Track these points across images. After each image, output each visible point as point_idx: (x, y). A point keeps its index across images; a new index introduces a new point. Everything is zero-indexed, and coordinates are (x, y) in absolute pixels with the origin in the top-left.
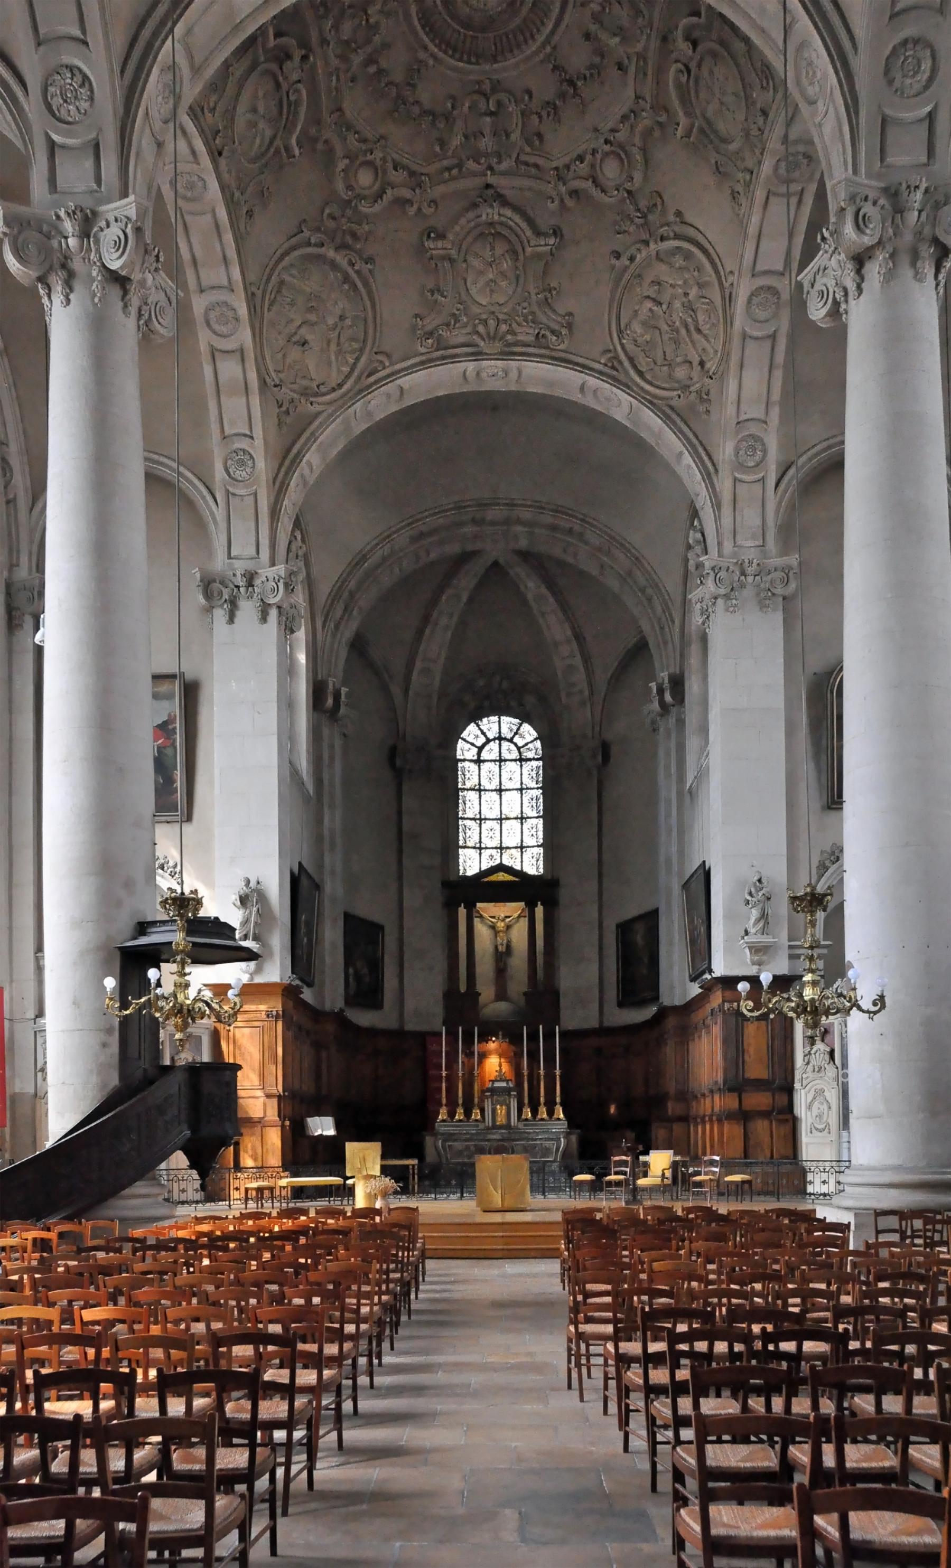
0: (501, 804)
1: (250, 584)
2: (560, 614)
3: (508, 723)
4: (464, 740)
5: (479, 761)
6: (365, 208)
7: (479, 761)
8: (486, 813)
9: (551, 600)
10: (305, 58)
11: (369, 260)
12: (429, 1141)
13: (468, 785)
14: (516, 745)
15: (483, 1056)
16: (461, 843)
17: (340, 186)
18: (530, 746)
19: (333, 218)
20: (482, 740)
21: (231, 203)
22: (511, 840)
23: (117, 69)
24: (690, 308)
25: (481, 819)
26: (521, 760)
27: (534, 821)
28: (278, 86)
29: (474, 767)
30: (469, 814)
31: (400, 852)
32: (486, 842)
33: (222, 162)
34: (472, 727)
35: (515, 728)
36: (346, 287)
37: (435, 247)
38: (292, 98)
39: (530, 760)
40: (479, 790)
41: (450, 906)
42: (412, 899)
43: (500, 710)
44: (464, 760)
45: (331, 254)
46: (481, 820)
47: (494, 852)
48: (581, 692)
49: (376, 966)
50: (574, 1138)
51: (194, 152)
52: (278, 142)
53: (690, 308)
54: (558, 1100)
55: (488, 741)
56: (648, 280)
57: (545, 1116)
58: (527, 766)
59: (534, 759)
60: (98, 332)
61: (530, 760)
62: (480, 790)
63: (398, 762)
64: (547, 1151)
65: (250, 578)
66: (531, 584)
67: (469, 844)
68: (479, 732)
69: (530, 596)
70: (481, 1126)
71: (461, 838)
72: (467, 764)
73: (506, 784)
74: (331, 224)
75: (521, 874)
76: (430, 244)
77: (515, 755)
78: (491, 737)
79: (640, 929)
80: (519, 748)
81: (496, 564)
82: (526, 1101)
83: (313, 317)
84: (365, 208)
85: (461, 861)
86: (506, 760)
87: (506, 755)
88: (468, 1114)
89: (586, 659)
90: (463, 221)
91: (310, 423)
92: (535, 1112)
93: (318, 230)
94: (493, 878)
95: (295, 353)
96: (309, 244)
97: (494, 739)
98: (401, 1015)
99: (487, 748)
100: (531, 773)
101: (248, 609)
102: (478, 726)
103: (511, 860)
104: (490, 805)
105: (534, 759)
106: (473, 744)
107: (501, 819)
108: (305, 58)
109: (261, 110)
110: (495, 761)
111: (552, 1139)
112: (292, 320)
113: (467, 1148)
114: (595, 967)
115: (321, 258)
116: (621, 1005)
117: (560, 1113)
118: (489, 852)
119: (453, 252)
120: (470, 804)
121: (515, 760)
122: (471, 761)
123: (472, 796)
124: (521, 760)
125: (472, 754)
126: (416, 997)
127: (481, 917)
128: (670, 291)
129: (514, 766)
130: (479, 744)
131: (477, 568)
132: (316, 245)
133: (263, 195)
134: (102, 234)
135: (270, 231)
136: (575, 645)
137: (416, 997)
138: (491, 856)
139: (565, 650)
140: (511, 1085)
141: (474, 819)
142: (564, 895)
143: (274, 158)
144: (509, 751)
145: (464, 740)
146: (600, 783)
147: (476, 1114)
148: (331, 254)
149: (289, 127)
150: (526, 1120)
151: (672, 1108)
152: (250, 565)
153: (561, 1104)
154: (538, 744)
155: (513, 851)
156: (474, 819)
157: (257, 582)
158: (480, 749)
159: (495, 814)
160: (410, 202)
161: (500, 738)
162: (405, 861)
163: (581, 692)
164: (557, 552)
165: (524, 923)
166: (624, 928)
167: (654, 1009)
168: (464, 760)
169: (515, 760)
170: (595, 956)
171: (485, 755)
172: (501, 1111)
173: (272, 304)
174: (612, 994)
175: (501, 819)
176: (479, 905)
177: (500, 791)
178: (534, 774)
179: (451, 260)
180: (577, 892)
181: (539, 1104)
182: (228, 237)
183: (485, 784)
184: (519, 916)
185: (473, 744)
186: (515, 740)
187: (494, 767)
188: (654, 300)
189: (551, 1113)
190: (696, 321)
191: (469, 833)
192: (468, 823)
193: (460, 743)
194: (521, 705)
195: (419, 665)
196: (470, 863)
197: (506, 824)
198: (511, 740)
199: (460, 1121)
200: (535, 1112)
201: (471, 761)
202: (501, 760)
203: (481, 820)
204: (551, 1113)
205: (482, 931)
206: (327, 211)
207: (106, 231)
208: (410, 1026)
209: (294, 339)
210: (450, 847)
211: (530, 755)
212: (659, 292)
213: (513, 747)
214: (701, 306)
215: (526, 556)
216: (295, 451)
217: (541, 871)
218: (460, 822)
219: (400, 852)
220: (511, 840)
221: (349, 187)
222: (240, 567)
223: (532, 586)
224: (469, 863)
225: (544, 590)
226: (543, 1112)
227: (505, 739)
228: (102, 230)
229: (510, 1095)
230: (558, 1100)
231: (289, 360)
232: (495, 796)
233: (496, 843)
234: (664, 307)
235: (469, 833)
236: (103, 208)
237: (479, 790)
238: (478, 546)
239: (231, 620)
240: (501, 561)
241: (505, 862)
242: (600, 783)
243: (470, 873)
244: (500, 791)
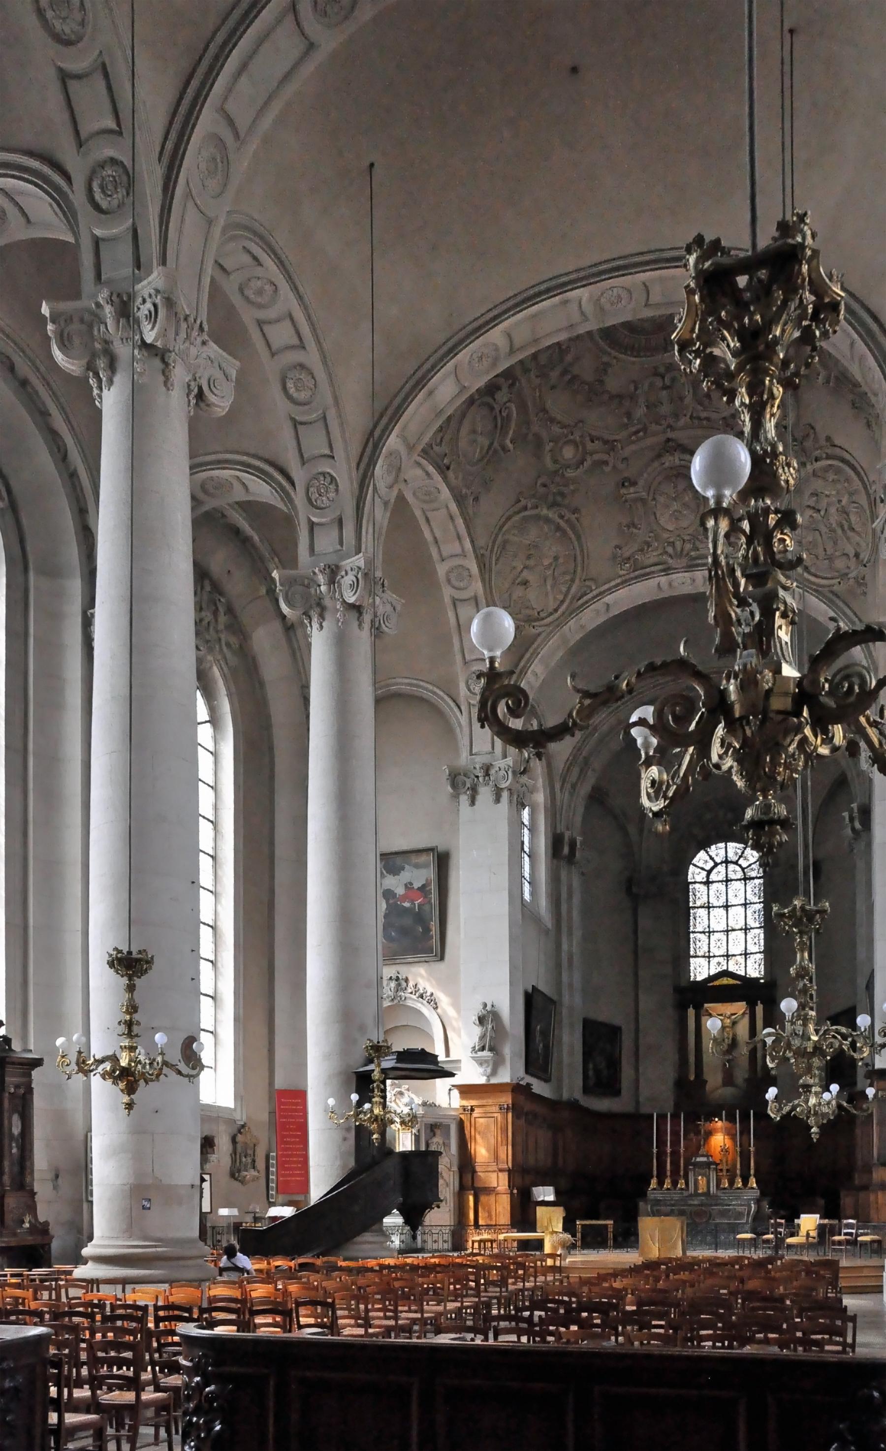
0: (726, 919)
1: (487, 774)
6: (570, 473)
8: (714, 926)
10: (512, 386)
11: (576, 511)
16: (692, 953)
17: (548, 460)
18: (753, 866)
19: (545, 486)
21: (460, 499)
23: (354, 465)
24: (845, 512)
25: (709, 932)
28: (492, 409)
30: (699, 928)
32: (714, 951)
33: (451, 474)
36: (558, 534)
37: (630, 492)
38: (504, 414)
40: (708, 907)
42: (646, 1002)
45: (545, 512)
46: (709, 933)
51: (428, 474)
52: (496, 444)
53: (845, 512)
56: (807, 494)
58: (750, 885)
60: (341, 645)
62: (709, 908)
65: (487, 769)
71: (692, 949)
74: (542, 490)
76: (623, 491)
83: (531, 562)
84: (570, 473)
85: (692, 968)
86: (731, 880)
90: (650, 469)
91: (535, 640)
93: (534, 496)
95: (518, 592)
96: (525, 508)
101: (485, 794)
107: (727, 931)
108: (512, 386)
109: (479, 430)
112: (514, 568)
115: (538, 517)
119: (644, 494)
120: (699, 920)
123: (702, 912)
124: (746, 879)
126: (650, 1083)
128: (826, 500)
129: (739, 885)
132: (532, 508)
133: (486, 484)
134: (342, 581)
135: (493, 506)
137: (650, 1083)
141: (704, 932)
143: (492, 456)
148: (545, 512)
149: (504, 433)
152: (485, 759)
156: (704, 932)
157: (492, 772)
159: (723, 927)
160: (606, 463)
162: (641, 973)
173: (497, 560)
175: (727, 931)
177: (727, 907)
179: (643, 501)
182: (460, 521)
183: (713, 901)
187: (722, 887)
188: (814, 508)
190: (849, 521)
192: (699, 936)
196: (700, 970)
197: (732, 935)
203: (709, 933)
206: (539, 482)
207: (346, 578)
209: (519, 580)
210: (681, 956)
212: (817, 502)
214: (852, 509)
216: (522, 664)
218: (692, 936)
221: (555, 462)
222: (479, 761)
224: (699, 969)
228: (343, 577)
231: (514, 597)
232: (722, 911)
233: (723, 951)
234: (822, 513)
235: (699, 943)
236: (343, 563)
239: (473, 802)
243: (699, 979)
244: (727, 907)
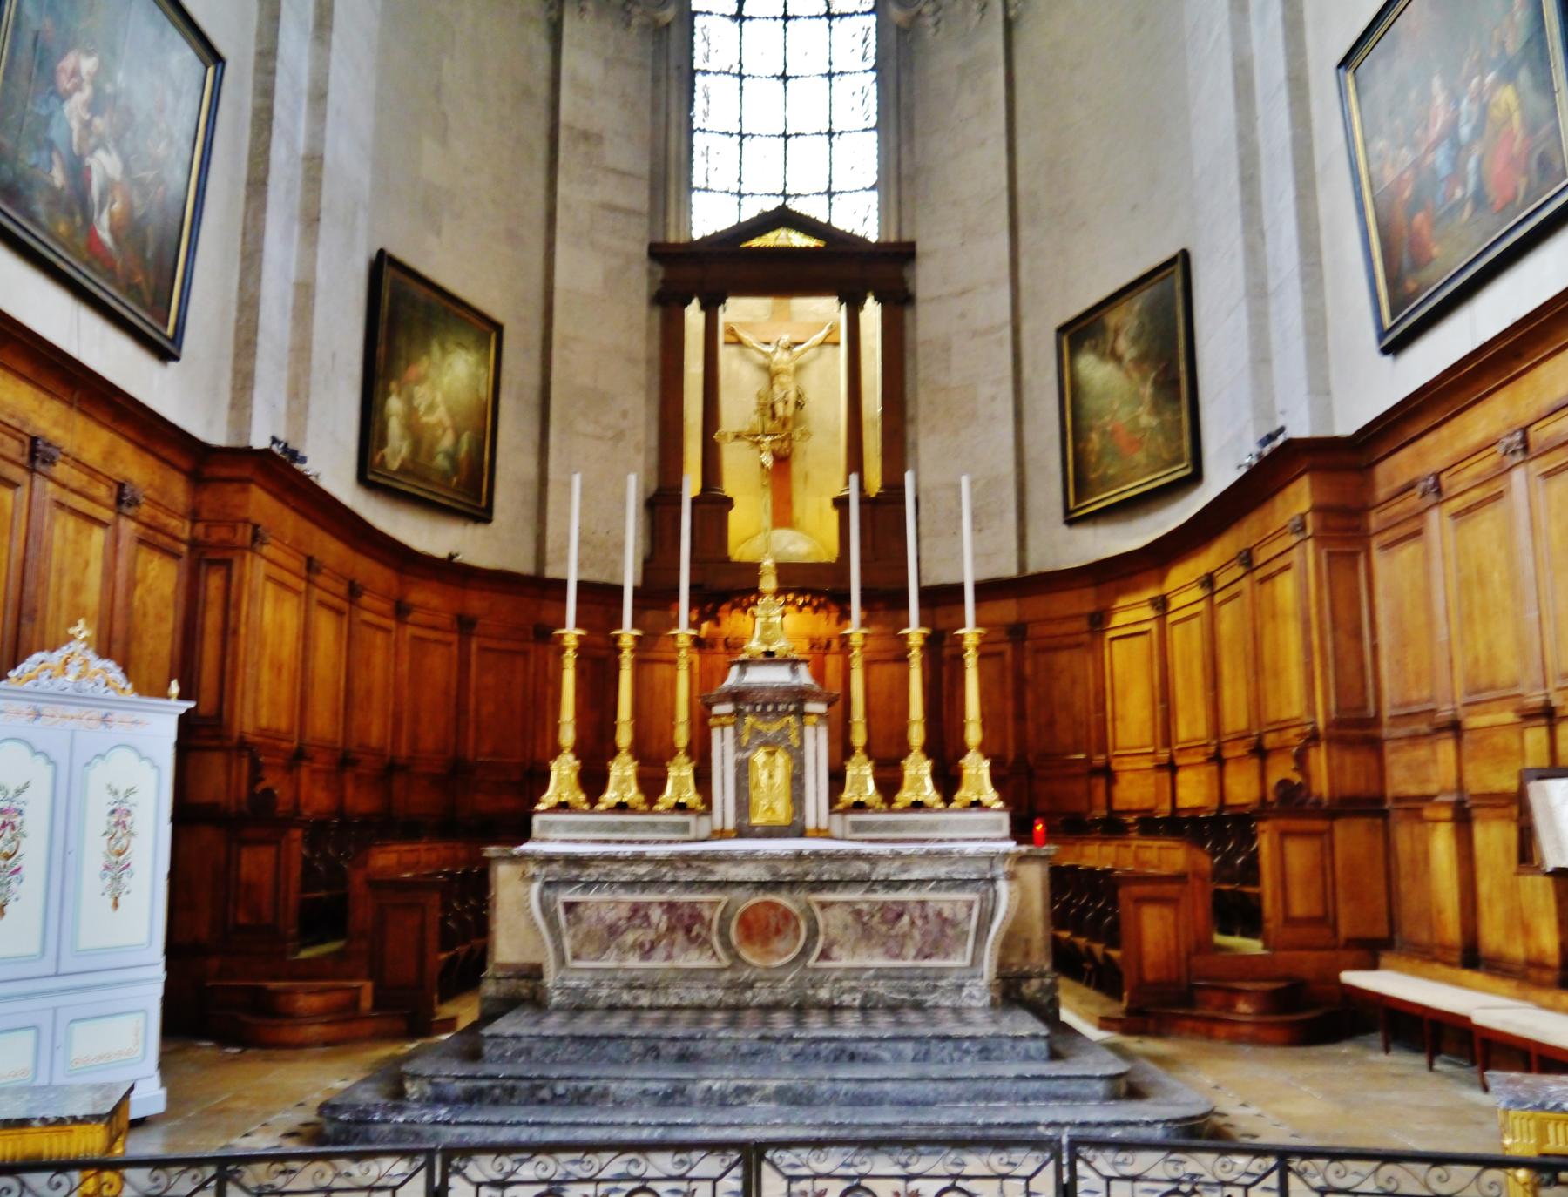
54: (973, 734)
57: (929, 793)
70: (702, 826)
82: (859, 738)
88: (651, 784)
92: (889, 784)
117: (976, 771)
140: (804, 677)
147: (679, 779)
150: (859, 806)
153: (984, 749)
172: (770, 773)
181: (905, 750)
189: (948, 781)
199: (622, 807)
200: (889, 784)
204: (948, 781)
226: (918, 773)
229: (800, 714)
230: (973, 734)
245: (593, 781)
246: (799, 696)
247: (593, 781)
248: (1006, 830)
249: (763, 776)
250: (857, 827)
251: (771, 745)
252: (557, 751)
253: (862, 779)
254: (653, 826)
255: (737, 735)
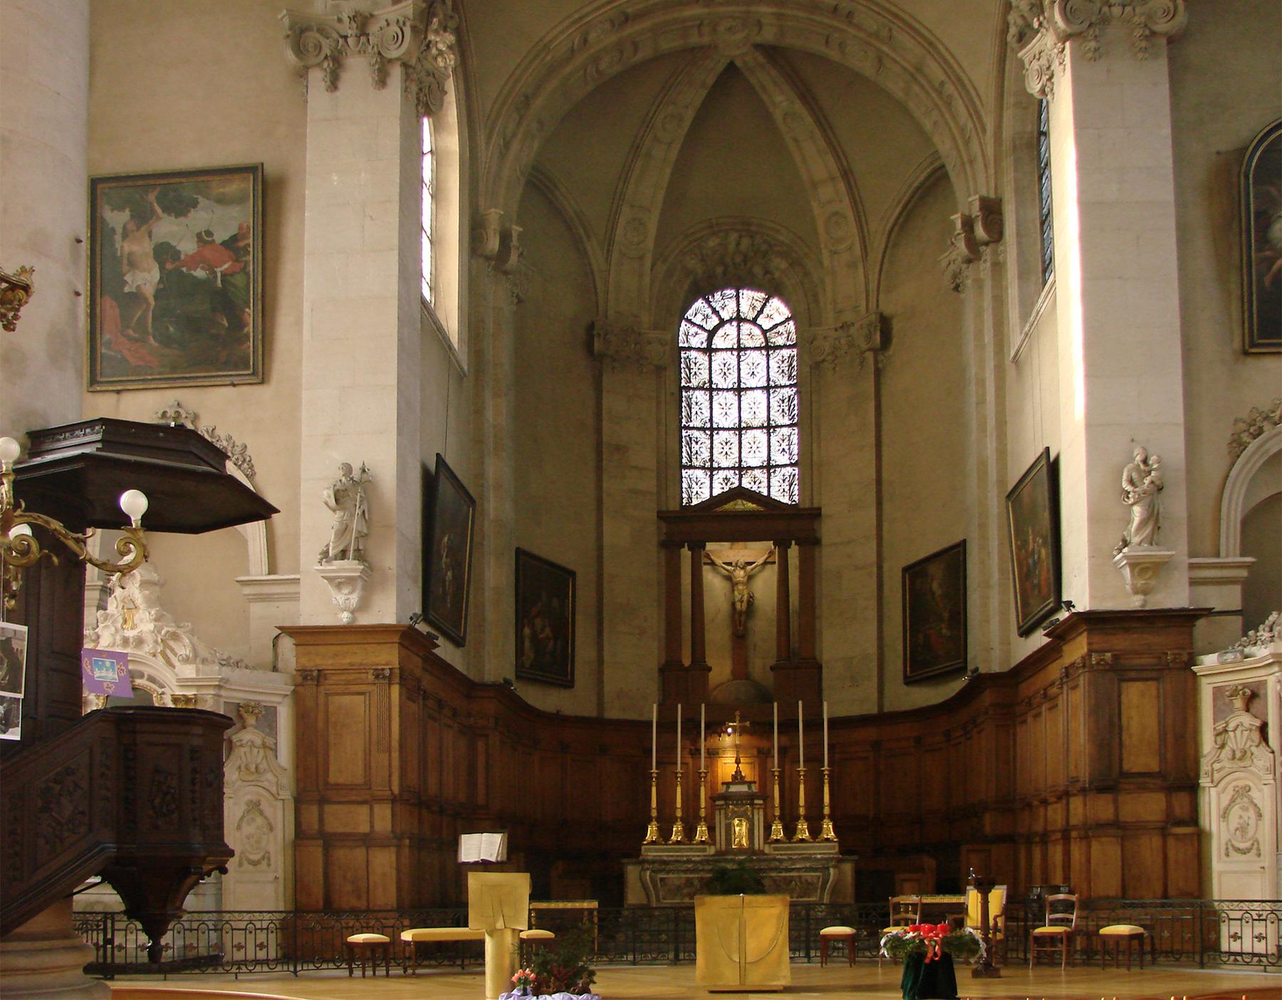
2: (822, 143)
3: (750, 298)
4: (689, 321)
5: (709, 350)
7: (709, 350)
9: (809, 120)
12: (632, 872)
13: (694, 383)
14: (760, 327)
15: (713, 754)
18: (781, 329)
20: (715, 321)
22: (754, 458)
25: (712, 429)
26: (768, 348)
27: (785, 431)
29: (702, 359)
30: (696, 423)
31: (599, 469)
32: (720, 460)
34: (700, 304)
35: (759, 306)
39: (780, 347)
40: (711, 389)
41: (670, 545)
43: (740, 284)
44: (690, 349)
46: (712, 430)
47: (730, 474)
48: (850, 249)
49: (563, 630)
50: (848, 868)
55: (722, 323)
58: (776, 356)
59: (785, 346)
61: (780, 347)
62: (711, 390)
63: (597, 346)
64: (808, 888)
66: (779, 98)
67: (695, 463)
68: (709, 311)
69: (778, 115)
72: (693, 354)
73: (748, 381)
75: (767, 501)
77: (759, 341)
78: (726, 318)
79: (936, 570)
80: (764, 332)
81: (731, 66)
86: (746, 349)
87: (746, 342)
89: (857, 204)
92: (790, 831)
94: (729, 506)
97: (731, 320)
98: (600, 695)
99: (721, 332)
100: (779, 366)
102: (708, 302)
103: (754, 482)
104: (725, 411)
105: (785, 346)
106: (701, 327)
110: (731, 350)
111: (815, 870)
113: (689, 882)
114: (872, 628)
116: (908, 681)
118: (722, 474)
121: (759, 349)
122: (698, 349)
123: (701, 396)
124: (768, 348)
125: (699, 340)
126: (621, 672)
127: (713, 564)
129: (758, 357)
130: (710, 326)
131: (708, 74)
136: (842, 186)
137: (621, 672)
138: (727, 479)
139: (826, 192)
141: (703, 429)
142: (827, 531)
144: (750, 335)
145: (689, 321)
146: (878, 373)
147: (702, 832)
150: (777, 841)
151: (989, 823)
154: (791, 326)
155: (757, 472)
158: (712, 334)
159: (732, 421)
161: (739, 319)
163: (850, 249)
164: (817, 46)
165: (771, 573)
166: (915, 572)
167: (963, 681)
168: (690, 349)
169: (759, 349)
170: (873, 614)
171: (718, 342)
174: (896, 665)
176: (710, 546)
178: (785, 366)
180: (846, 528)
183: (718, 380)
184: (765, 563)
185: (701, 327)
186: (759, 321)
187: (731, 359)
191: (695, 447)
193: (684, 326)
194: (767, 272)
195: (626, 214)
198: (754, 321)
199: (678, 842)
200: (790, 831)
201: (698, 349)
202: (740, 349)
205: (713, 582)
208: (613, 713)
211: (780, 341)
213: (756, 331)
215: (772, 53)
217: (796, 498)
219: (599, 469)
220: (754, 458)
223: (781, 101)
224: (696, 488)
225: (798, 107)
227: (746, 320)
233: (732, 461)
237: (711, 389)
238: (706, 40)
240: (738, 63)
241: (745, 484)
242: (878, 373)
244: (739, 390)
245: (665, 833)
246: (751, 797)
247: (665, 833)
248: (837, 850)
249: (737, 829)
250: (776, 849)
251: (740, 816)
252: (650, 820)
253: (778, 830)
254: (691, 850)
255: (726, 814)
